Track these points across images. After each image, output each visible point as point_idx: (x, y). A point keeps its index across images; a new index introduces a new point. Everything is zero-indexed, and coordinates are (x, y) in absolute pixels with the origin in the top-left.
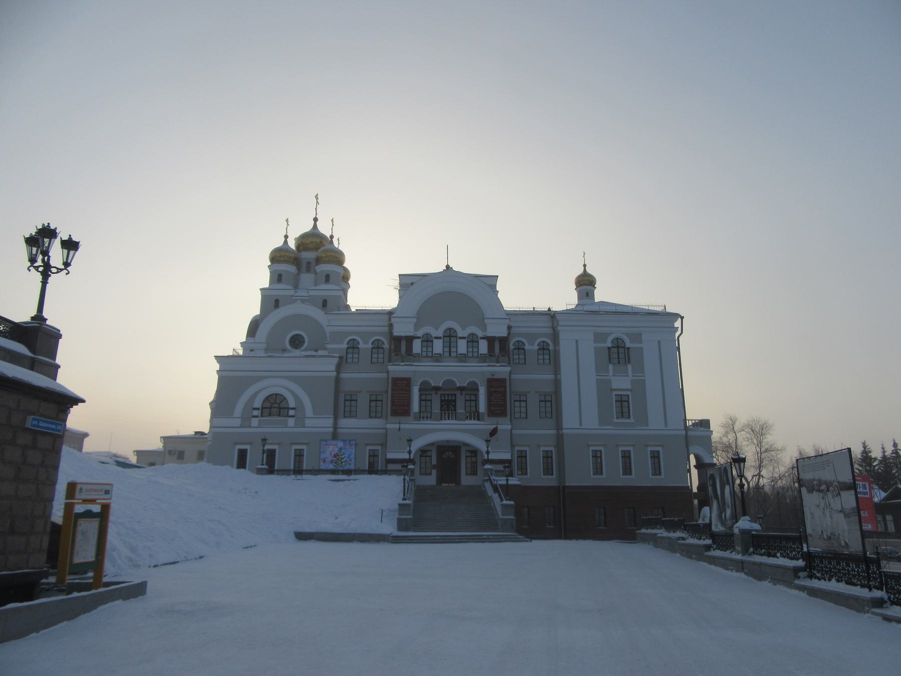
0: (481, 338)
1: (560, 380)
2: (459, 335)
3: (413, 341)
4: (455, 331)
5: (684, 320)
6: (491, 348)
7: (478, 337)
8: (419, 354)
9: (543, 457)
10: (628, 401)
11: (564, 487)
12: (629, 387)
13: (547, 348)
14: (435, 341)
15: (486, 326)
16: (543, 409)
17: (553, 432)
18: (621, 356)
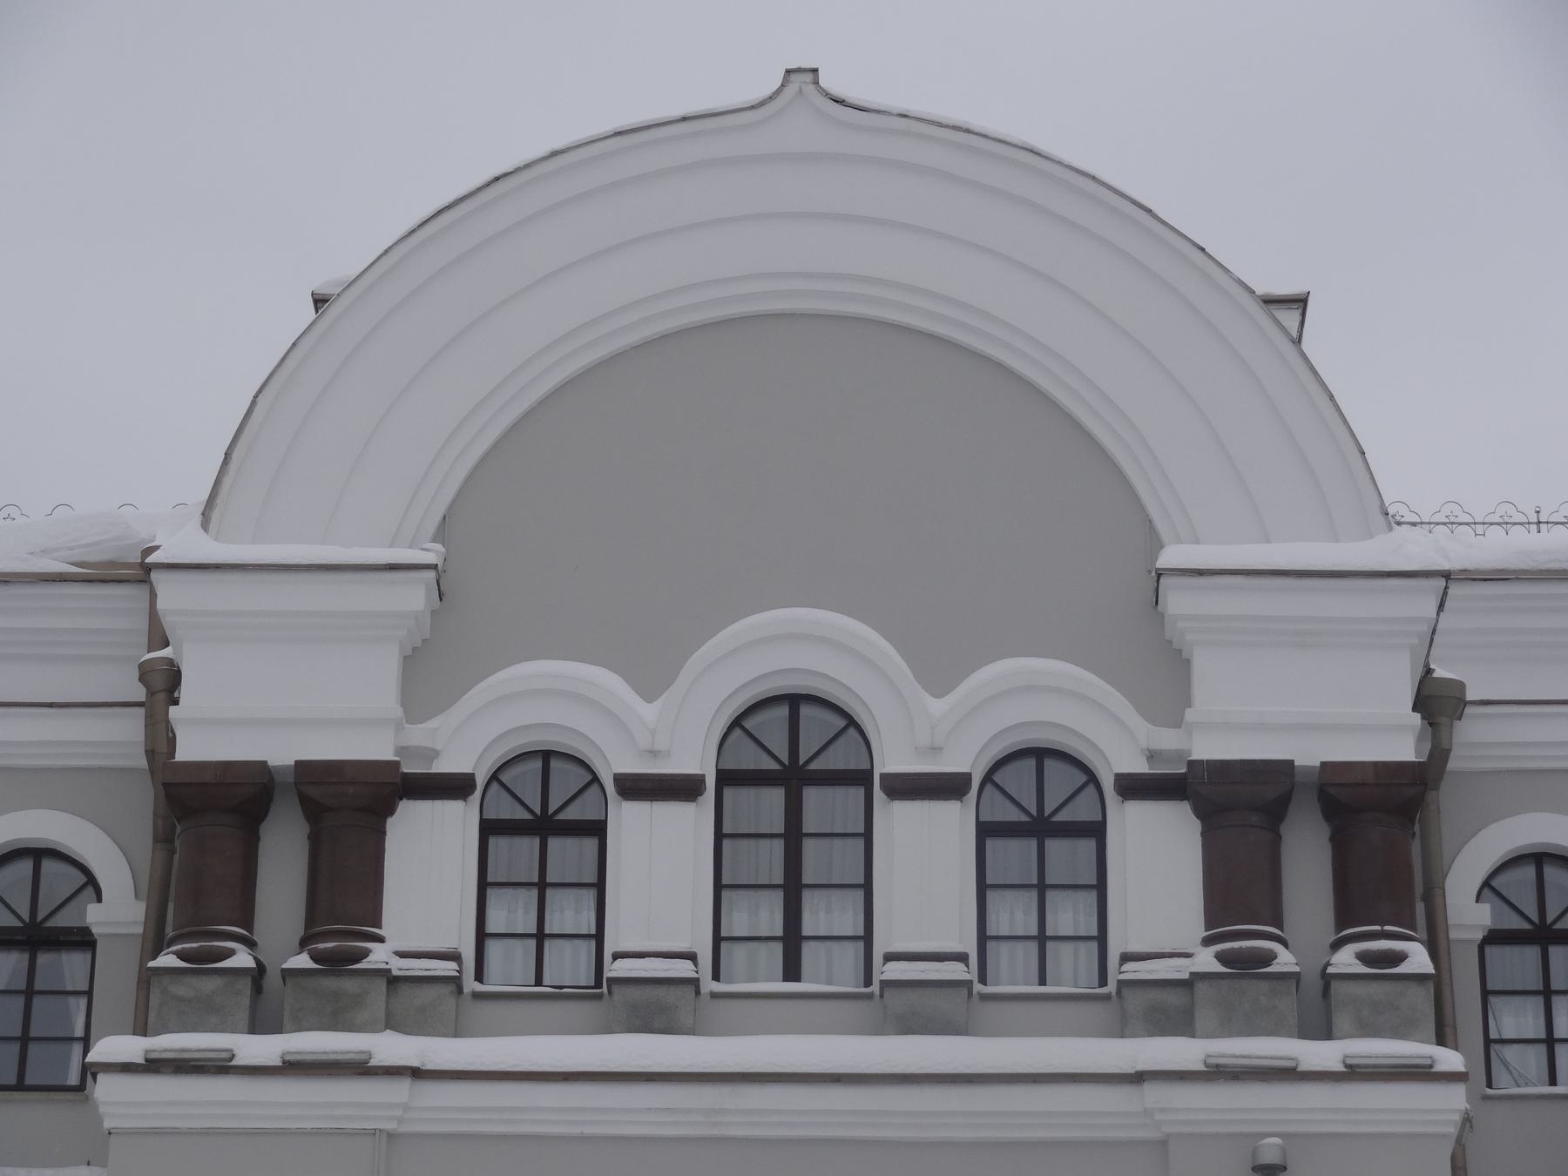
0: (1134, 787)
2: (892, 759)
3: (391, 823)
4: (851, 722)
8: (454, 957)
15: (1187, 664)
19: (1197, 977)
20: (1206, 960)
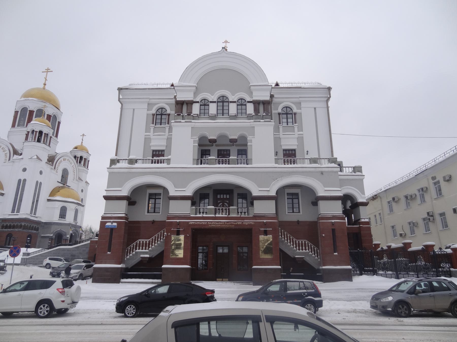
0: (249, 102)
4: (227, 98)
6: (256, 110)
7: (246, 101)
14: (211, 105)
15: (252, 93)
19: (253, 115)
20: (254, 114)
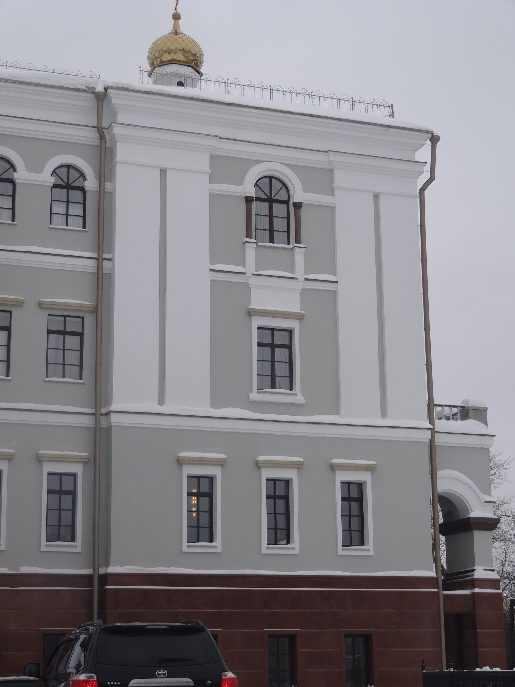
1: (111, 276)
5: (438, 145)
9: (49, 492)
10: (290, 347)
11: (105, 579)
12: (296, 309)
13: (77, 184)
16: (55, 356)
17: (87, 421)
18: (279, 224)
